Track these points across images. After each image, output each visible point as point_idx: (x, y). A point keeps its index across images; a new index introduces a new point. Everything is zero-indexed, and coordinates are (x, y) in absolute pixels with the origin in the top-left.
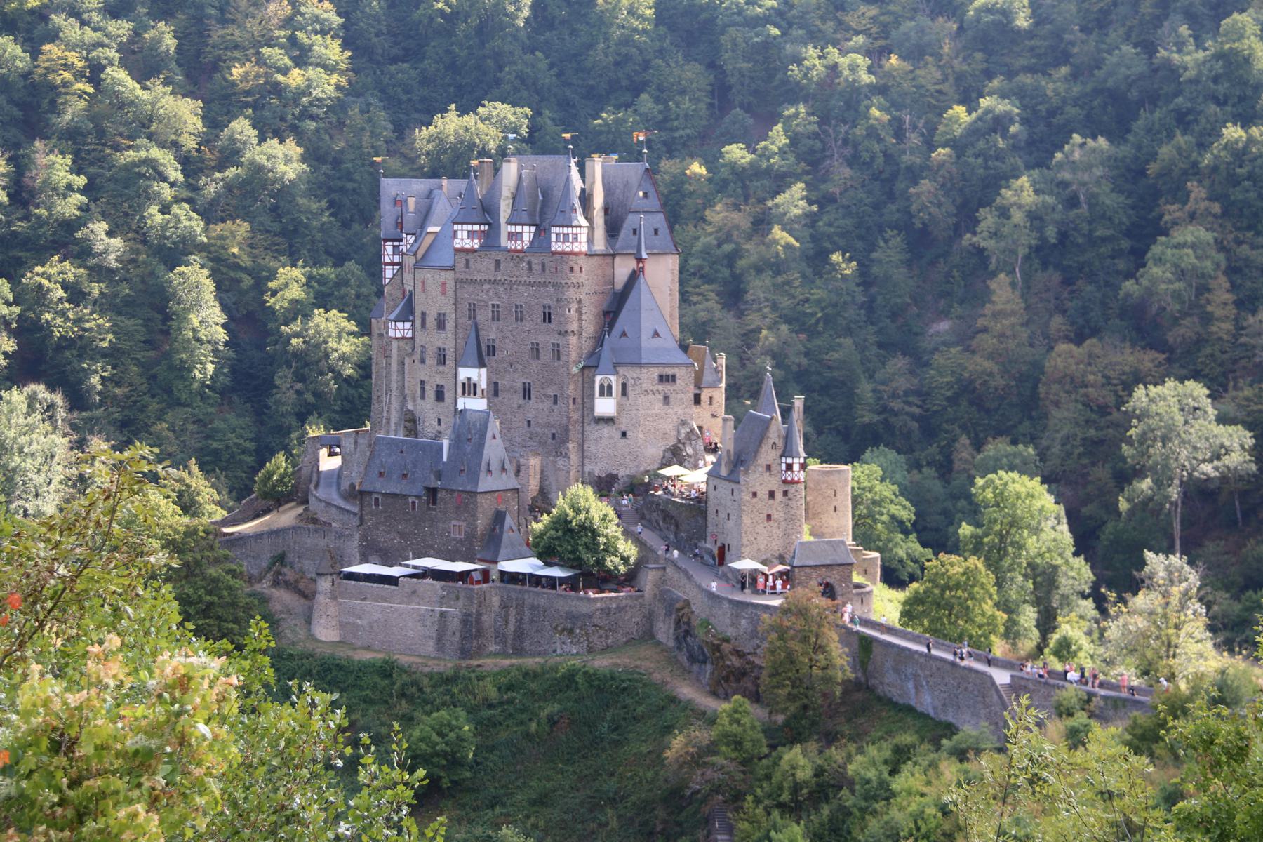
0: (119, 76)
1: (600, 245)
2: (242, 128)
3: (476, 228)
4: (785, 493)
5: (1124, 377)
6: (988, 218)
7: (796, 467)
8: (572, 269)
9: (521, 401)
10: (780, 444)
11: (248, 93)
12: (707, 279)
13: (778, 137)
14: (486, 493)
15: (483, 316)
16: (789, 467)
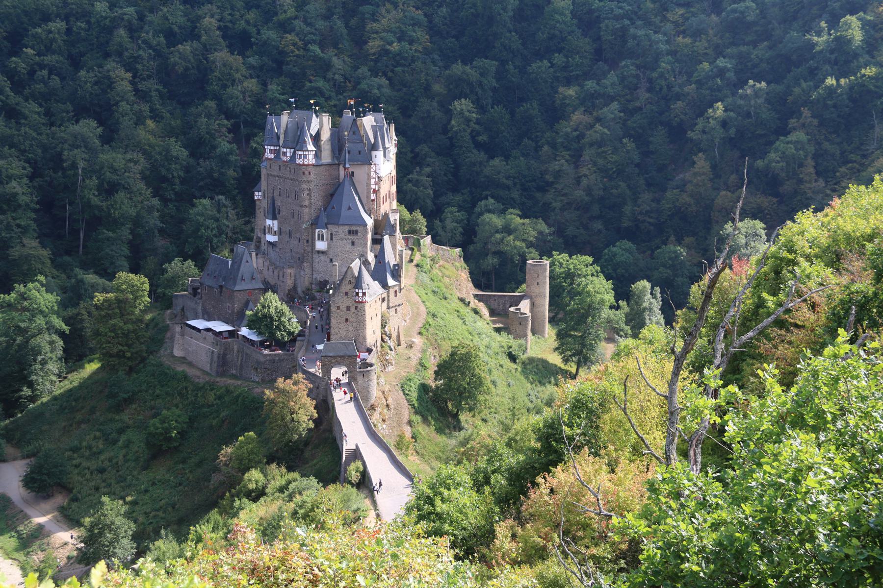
0: (315, 49)
1: (326, 157)
2: (364, 70)
3: (272, 148)
4: (356, 308)
5: (753, 210)
6: (701, 122)
7: (361, 294)
8: (304, 173)
9: (289, 239)
10: (353, 281)
11: (374, 54)
12: (567, 148)
13: (612, 77)
14: (240, 291)
15: (276, 193)
16: (357, 294)
